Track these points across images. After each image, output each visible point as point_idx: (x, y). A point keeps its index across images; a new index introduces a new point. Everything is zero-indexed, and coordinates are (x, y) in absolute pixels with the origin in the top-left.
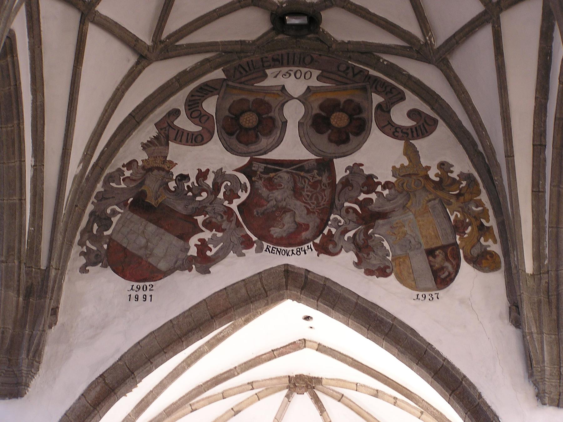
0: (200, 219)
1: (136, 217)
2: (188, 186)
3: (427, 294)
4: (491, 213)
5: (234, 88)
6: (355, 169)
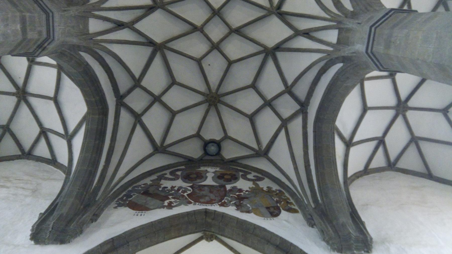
0: (170, 197)
4: (291, 198)
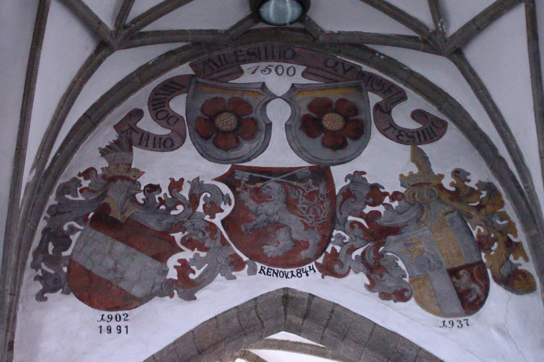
0: (178, 236)
1: (100, 235)
2: (160, 198)
3: (454, 320)
4: (518, 226)
5: (205, 85)
6: (357, 178)
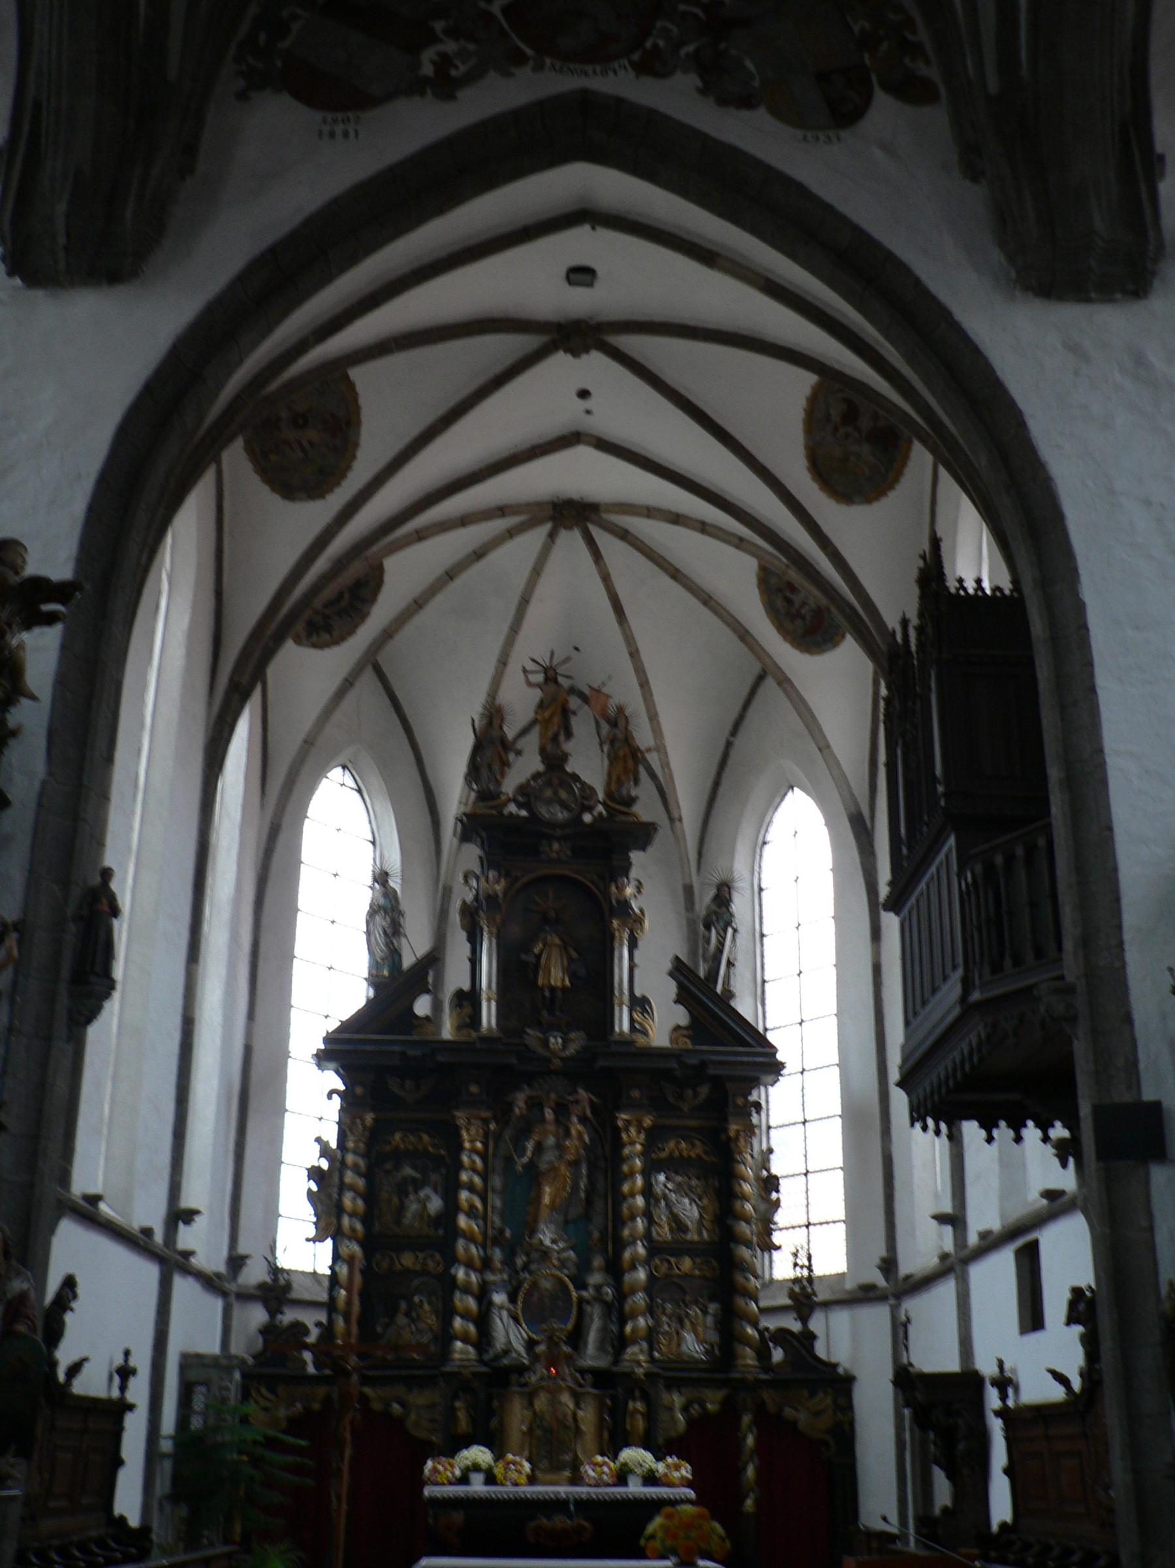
0: (439, 26)
